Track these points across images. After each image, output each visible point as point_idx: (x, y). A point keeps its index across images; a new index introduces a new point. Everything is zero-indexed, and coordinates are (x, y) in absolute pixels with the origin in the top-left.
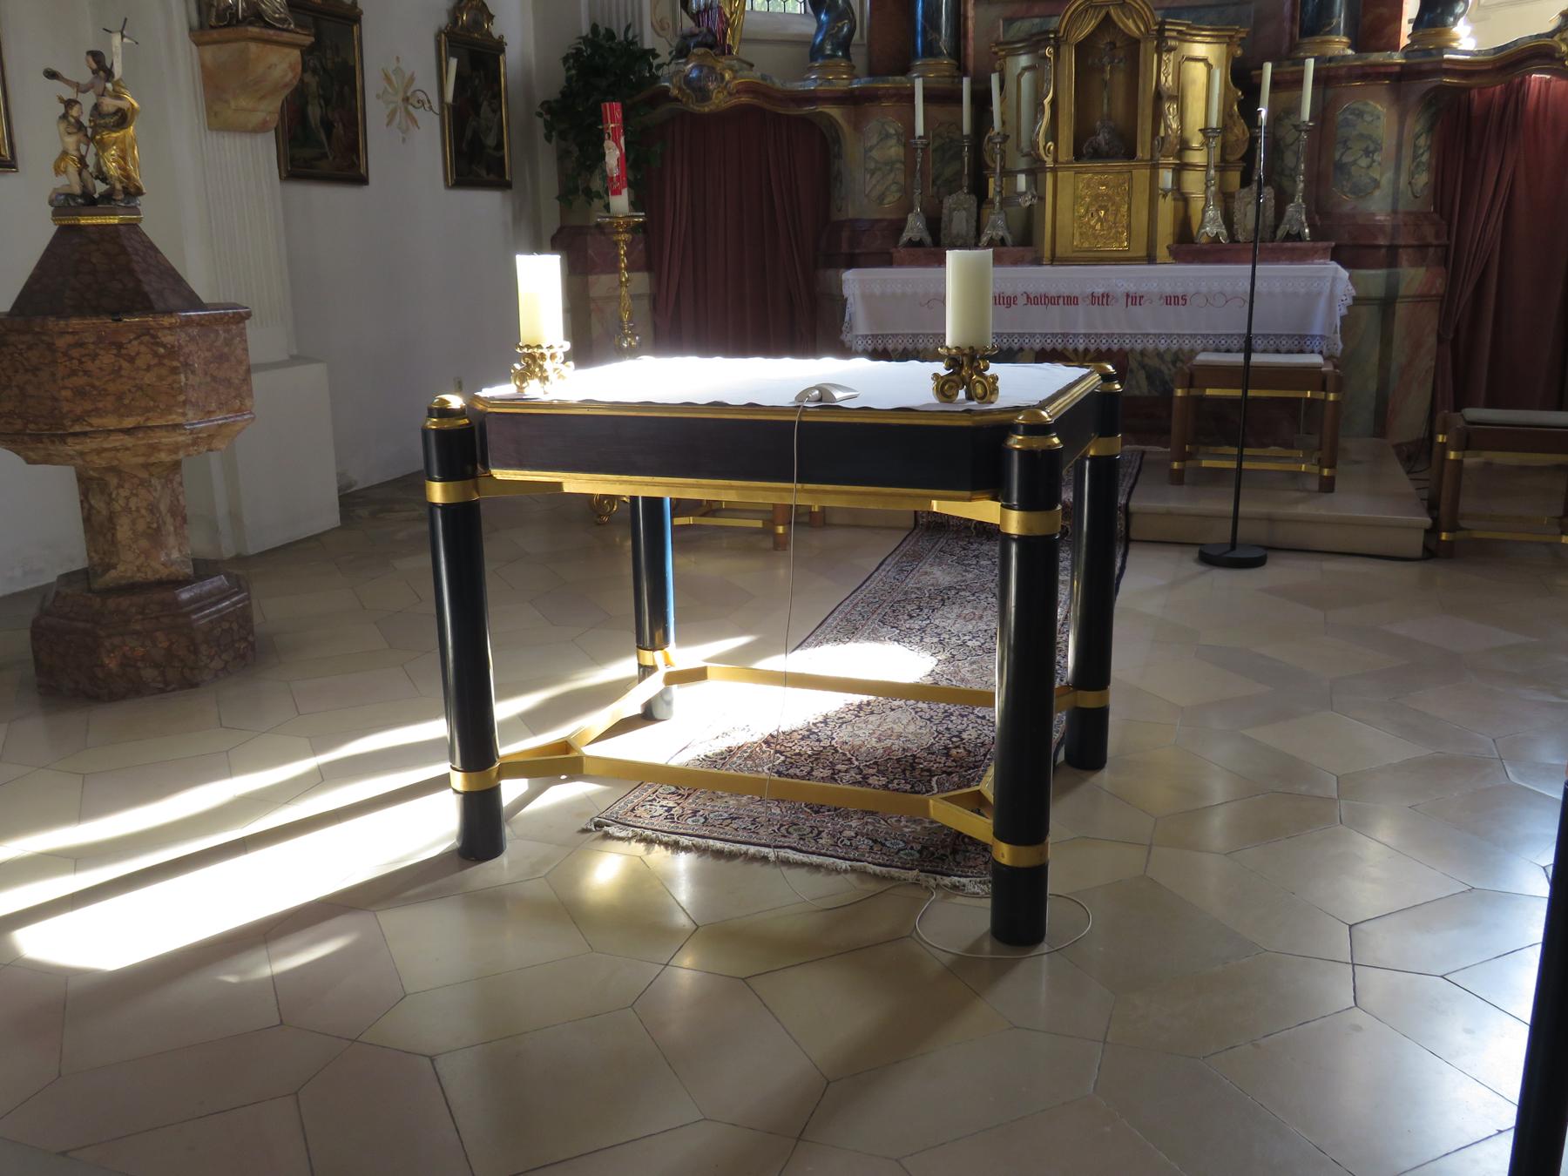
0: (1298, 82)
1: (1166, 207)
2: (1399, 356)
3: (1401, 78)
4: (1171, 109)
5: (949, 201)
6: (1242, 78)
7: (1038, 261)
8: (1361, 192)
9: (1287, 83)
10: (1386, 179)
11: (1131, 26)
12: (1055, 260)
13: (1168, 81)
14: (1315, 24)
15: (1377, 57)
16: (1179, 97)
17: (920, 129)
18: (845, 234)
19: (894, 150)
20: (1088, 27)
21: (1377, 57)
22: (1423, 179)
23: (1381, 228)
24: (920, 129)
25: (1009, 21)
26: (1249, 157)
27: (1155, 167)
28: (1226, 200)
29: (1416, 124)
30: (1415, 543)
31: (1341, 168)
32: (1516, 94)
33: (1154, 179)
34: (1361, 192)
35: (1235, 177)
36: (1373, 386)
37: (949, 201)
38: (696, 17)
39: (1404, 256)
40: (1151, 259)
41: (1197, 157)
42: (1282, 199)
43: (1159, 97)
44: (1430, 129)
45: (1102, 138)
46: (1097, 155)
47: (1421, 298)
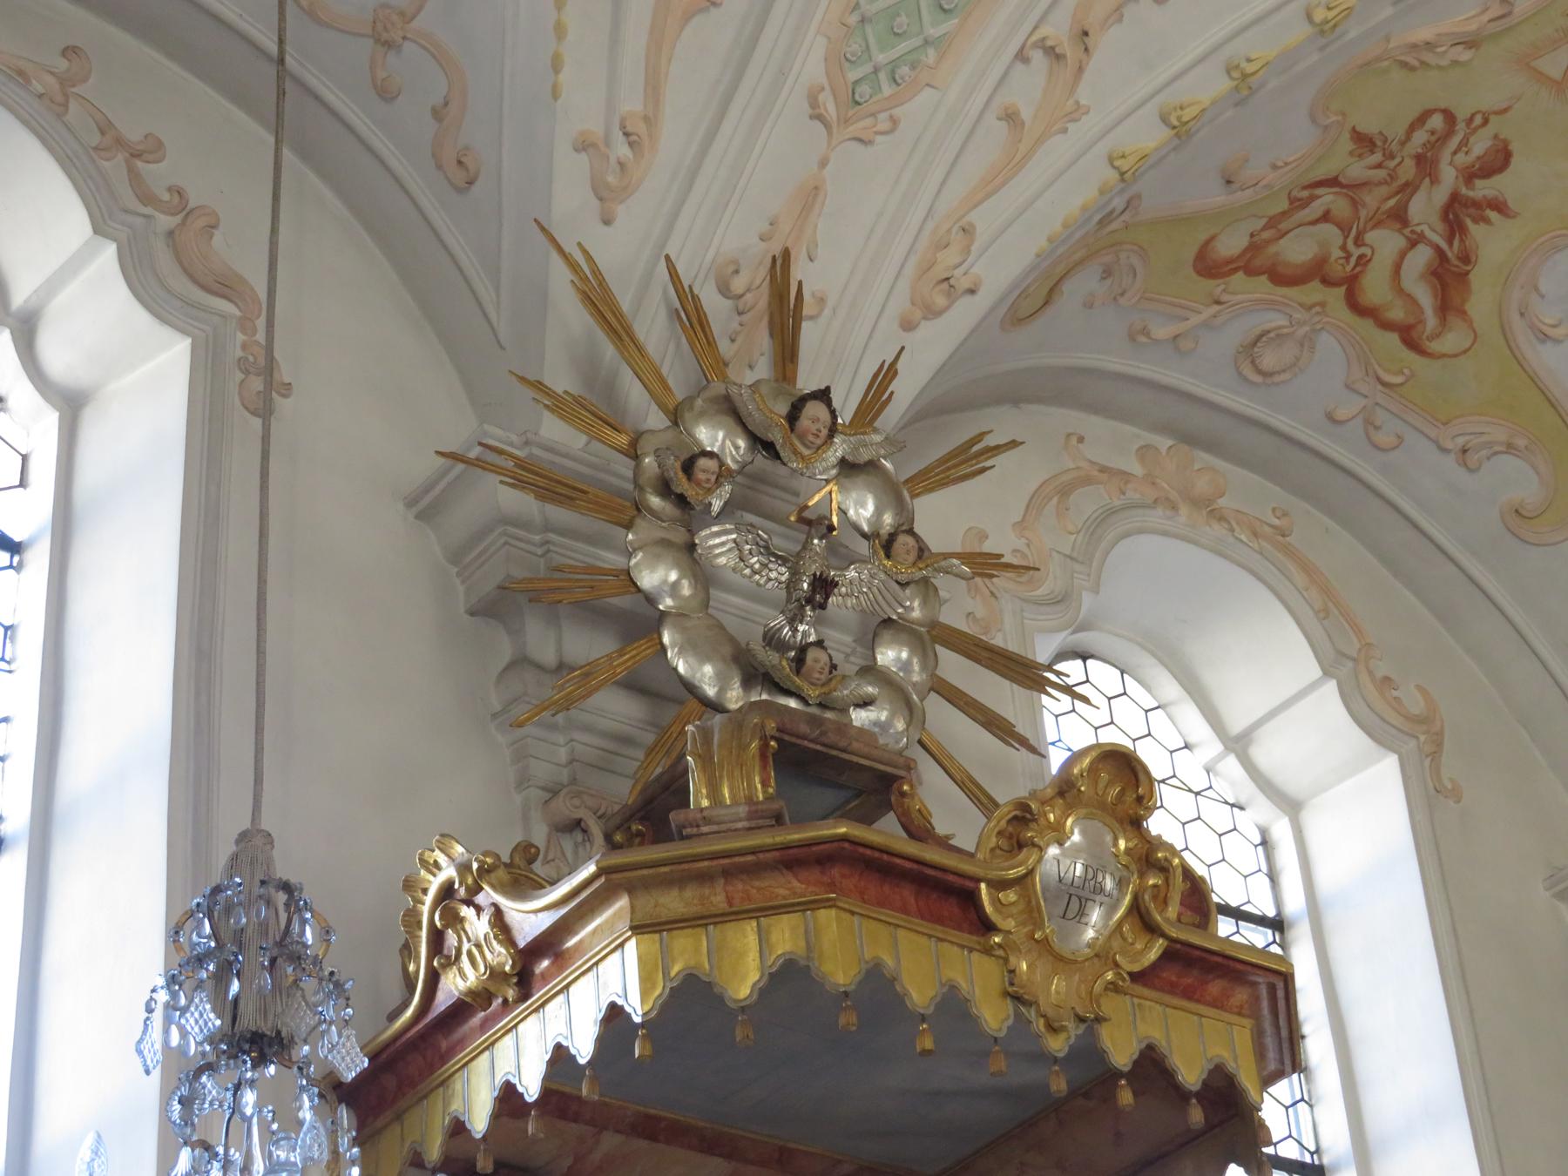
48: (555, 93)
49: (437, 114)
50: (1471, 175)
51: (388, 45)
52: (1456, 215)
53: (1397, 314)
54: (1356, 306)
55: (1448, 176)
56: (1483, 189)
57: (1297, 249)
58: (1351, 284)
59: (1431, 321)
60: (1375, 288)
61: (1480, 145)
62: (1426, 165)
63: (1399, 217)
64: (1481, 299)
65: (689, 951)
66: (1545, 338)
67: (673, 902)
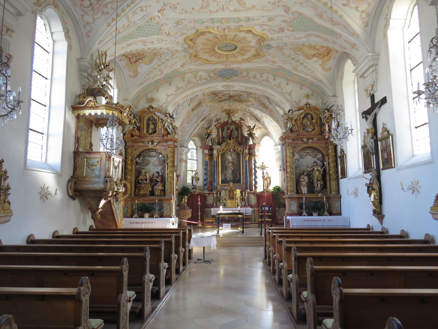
0: (246, 193)
1: (236, 203)
2: (256, 215)
3: (254, 193)
4: (236, 195)
5: (217, 202)
6: (241, 193)
7: (226, 208)
8: (251, 202)
9: (245, 193)
10: (253, 201)
11: (233, 189)
12: (227, 208)
13: (236, 193)
14: (247, 189)
15: (252, 192)
16: (237, 194)
17: (215, 196)
18: (208, 205)
19: (212, 198)
20: (229, 189)
21: (252, 192)
22: (256, 201)
23: (253, 205)
24: (215, 196)
25: (221, 187)
26: (242, 199)
27: (235, 200)
28: (241, 203)
29: (255, 197)
30: (258, 226)
31: (250, 200)
32: (262, 194)
33: (235, 201)
34: (251, 202)
35: (241, 201)
36: (254, 218)
37: (217, 202)
38: (193, 186)
39: (255, 207)
40: (235, 207)
41: (239, 199)
42: (245, 203)
43: (235, 194)
44: (256, 197)
45: (231, 197)
46: (230, 199)
47: (257, 211)
48: (100, 37)
49: (89, 31)
50: (142, 57)
51: (87, 24)
52: (139, 59)
53: (131, 62)
54: (129, 60)
55: (141, 57)
56: (142, 58)
57: (129, 56)
58: (130, 59)
59: (133, 63)
60: (131, 60)
61: (144, 56)
62: (140, 56)
63: (136, 57)
64: (137, 63)
65: (108, 111)
66: (139, 67)
67: (108, 108)
